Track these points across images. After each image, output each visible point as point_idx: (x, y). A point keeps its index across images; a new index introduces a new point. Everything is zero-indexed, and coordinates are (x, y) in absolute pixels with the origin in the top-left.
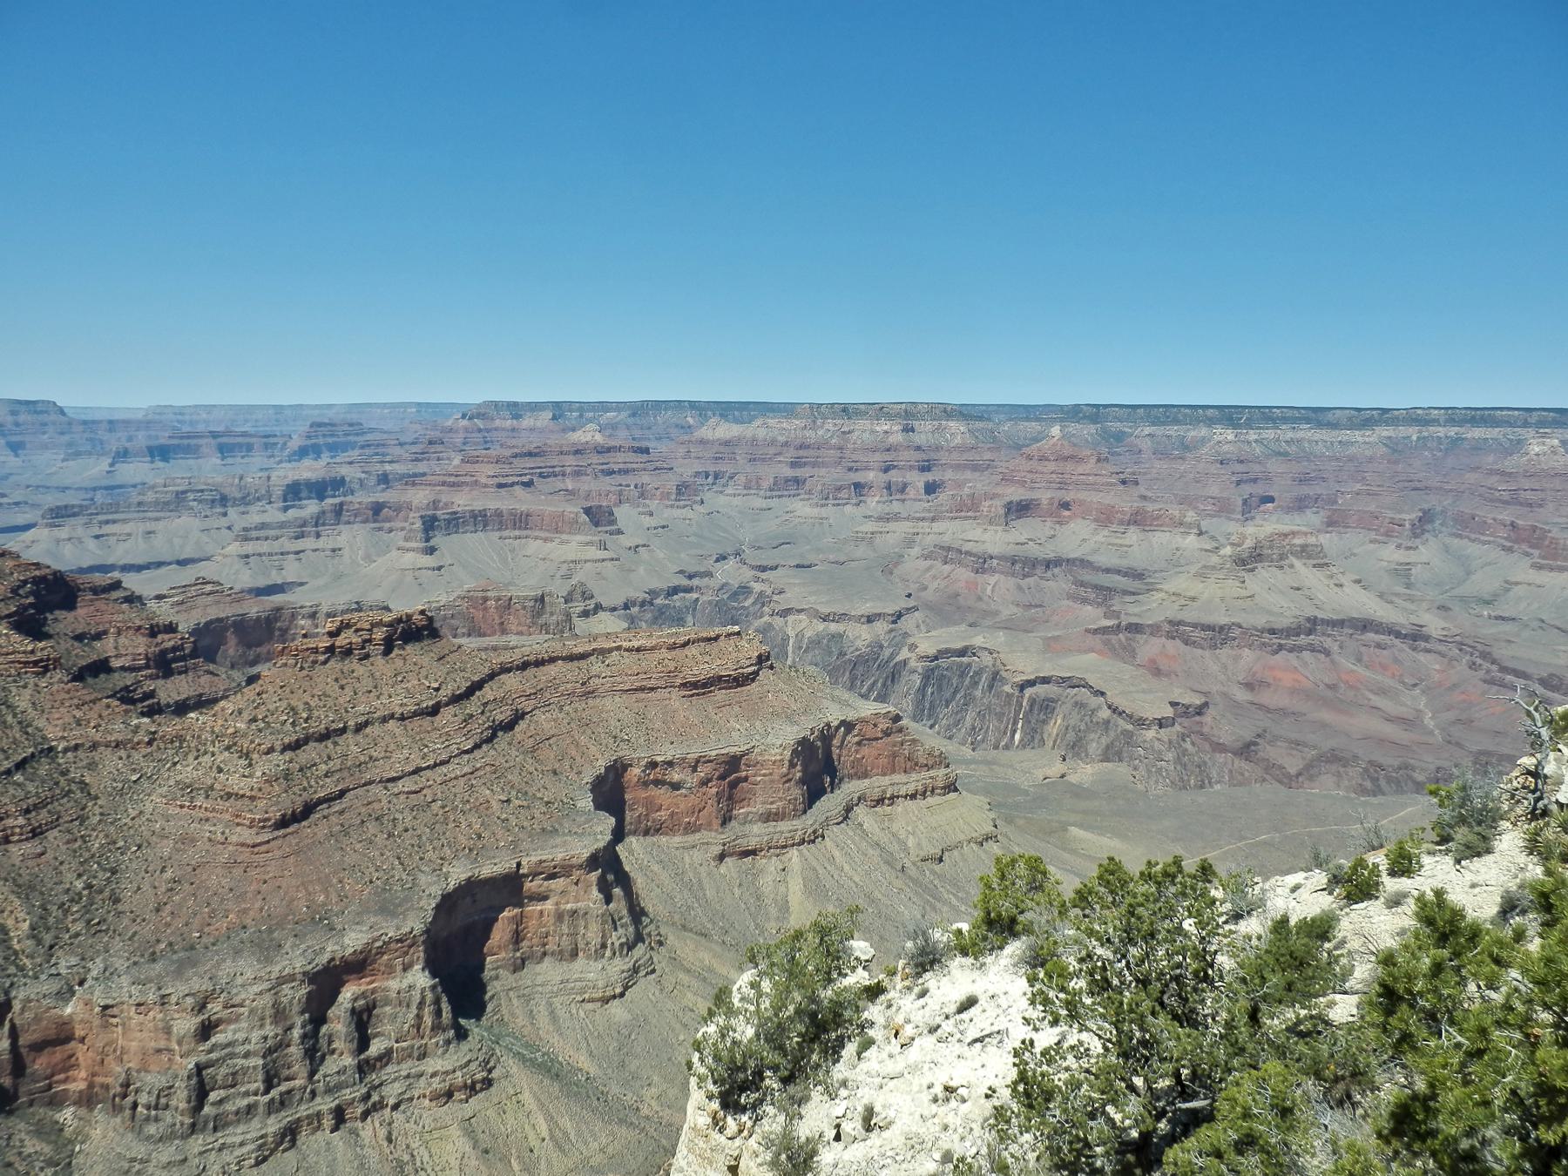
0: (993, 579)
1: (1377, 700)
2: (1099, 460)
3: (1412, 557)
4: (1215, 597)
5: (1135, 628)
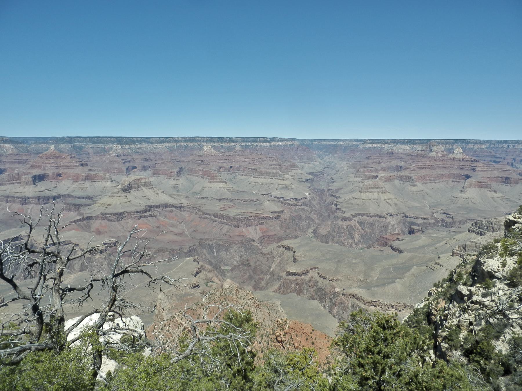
0: (30, 207)
1: (171, 229)
2: (71, 157)
3: (178, 182)
4: (116, 203)
5: (89, 218)
